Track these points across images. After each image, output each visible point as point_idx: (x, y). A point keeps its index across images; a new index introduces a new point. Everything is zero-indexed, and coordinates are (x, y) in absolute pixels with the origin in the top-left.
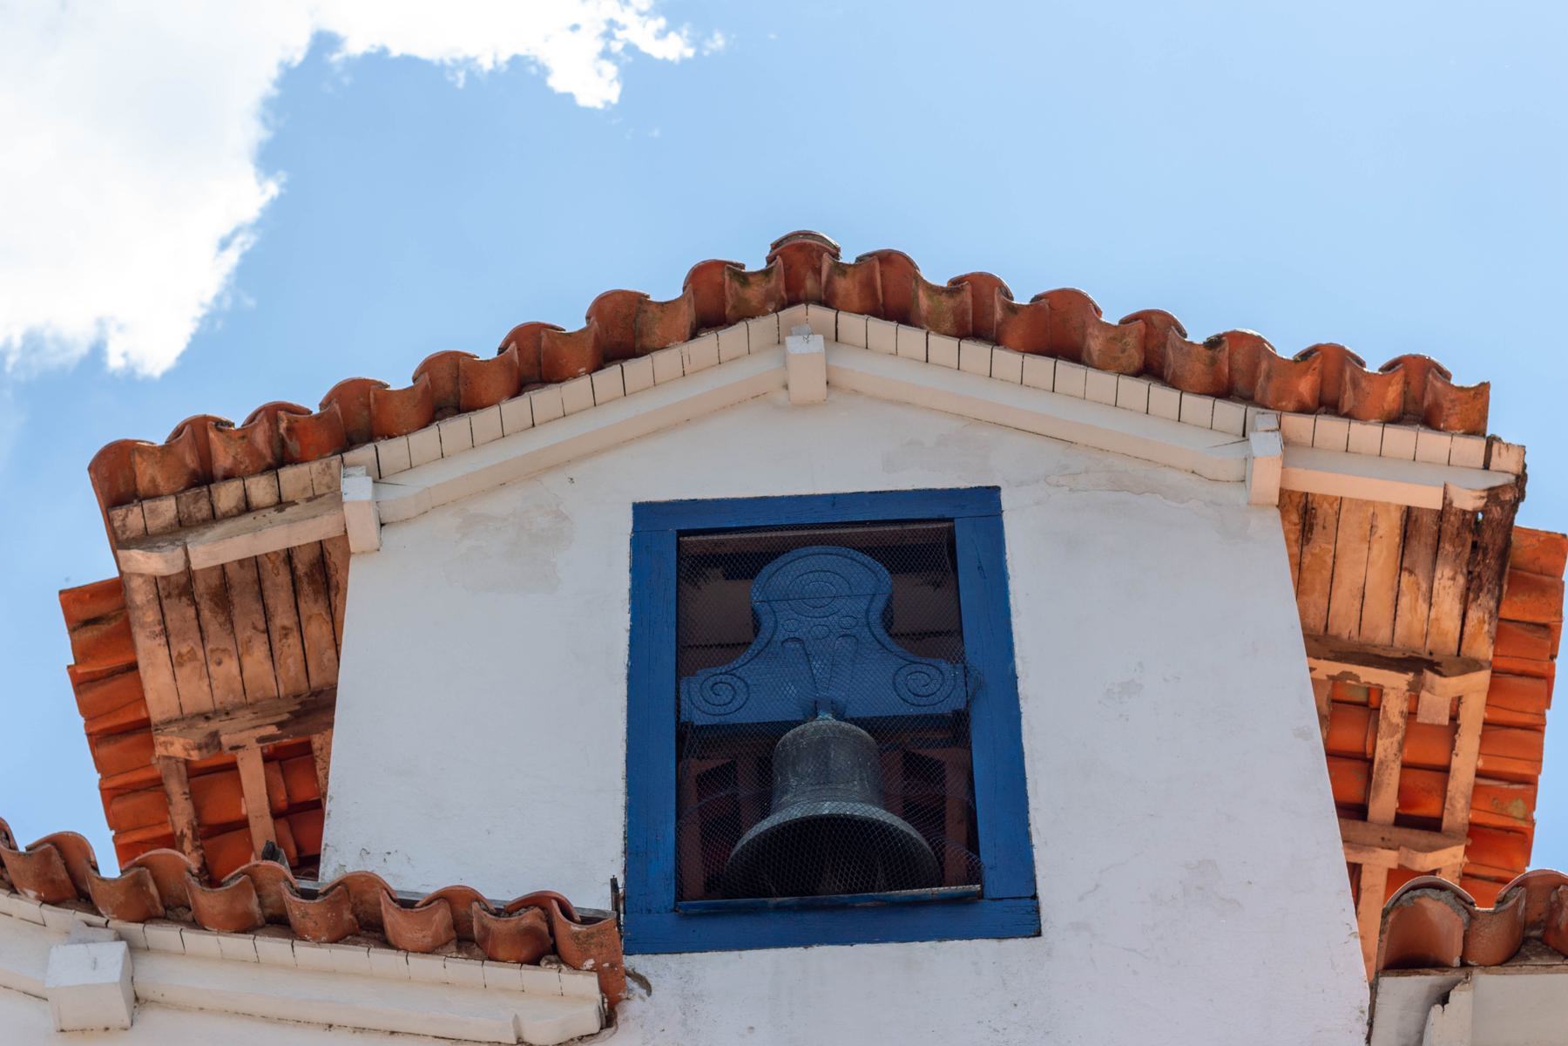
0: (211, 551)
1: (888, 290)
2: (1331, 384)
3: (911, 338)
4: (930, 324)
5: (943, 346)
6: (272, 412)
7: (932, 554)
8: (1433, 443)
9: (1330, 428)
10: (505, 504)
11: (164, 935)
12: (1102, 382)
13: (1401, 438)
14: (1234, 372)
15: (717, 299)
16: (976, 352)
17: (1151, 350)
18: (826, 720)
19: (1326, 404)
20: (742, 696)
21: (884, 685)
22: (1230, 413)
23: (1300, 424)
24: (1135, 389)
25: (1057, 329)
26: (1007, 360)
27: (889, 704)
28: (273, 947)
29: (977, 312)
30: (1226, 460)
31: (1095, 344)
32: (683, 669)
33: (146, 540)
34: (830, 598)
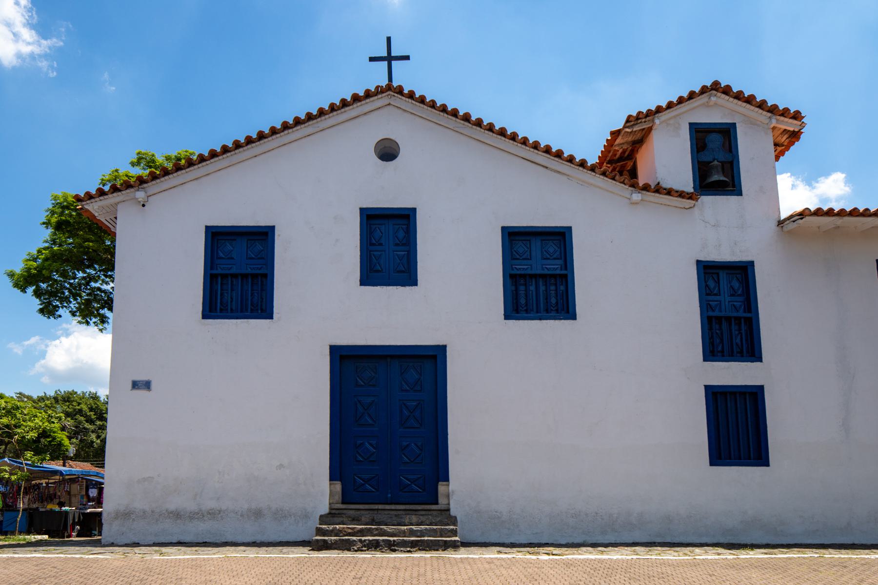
0: (636, 128)
1: (727, 91)
2: (785, 113)
3: (727, 97)
4: (731, 96)
5: (731, 99)
6: (649, 110)
7: (727, 132)
8: (795, 122)
9: (782, 118)
10: (672, 122)
11: (644, 192)
12: (752, 108)
13: (791, 121)
14: (773, 110)
15: (704, 90)
16: (736, 101)
17: (762, 105)
18: (716, 163)
19: (782, 115)
20: (706, 157)
21: (722, 156)
22: (769, 114)
23: (778, 117)
24: (757, 109)
25: (750, 100)
26: (740, 103)
27: (723, 160)
28: (657, 195)
29: (739, 96)
30: (767, 121)
31: (754, 103)
32: (698, 152)
33: (628, 127)
34: (715, 140)
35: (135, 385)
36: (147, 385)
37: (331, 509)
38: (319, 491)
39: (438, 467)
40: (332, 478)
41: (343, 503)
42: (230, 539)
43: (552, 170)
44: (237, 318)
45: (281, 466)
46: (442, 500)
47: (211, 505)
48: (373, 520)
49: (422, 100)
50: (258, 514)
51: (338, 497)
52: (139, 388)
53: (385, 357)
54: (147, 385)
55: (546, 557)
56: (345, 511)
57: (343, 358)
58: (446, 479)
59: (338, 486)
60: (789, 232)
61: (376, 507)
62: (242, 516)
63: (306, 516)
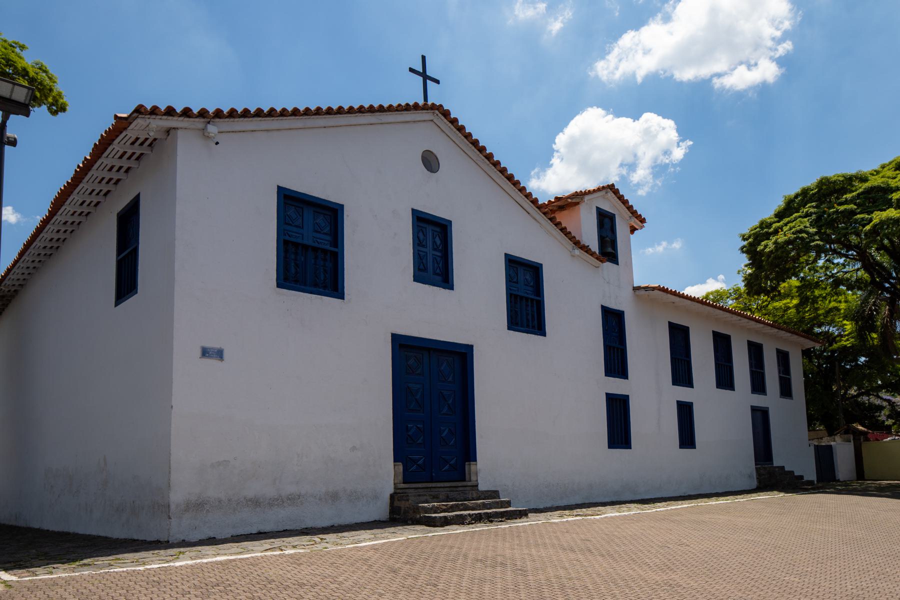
35: (205, 353)
36: (219, 354)
37: (395, 488)
38: (384, 474)
39: (468, 452)
40: (396, 459)
41: (404, 483)
42: (309, 524)
43: (532, 216)
44: (311, 293)
45: (354, 448)
46: (473, 478)
47: (289, 489)
48: (448, 497)
49: (461, 129)
50: (334, 497)
51: (401, 478)
52: (210, 357)
53: (429, 350)
54: (219, 354)
55: (570, 519)
56: (407, 491)
57: (401, 346)
58: (476, 461)
59: (400, 467)
60: (637, 296)
61: (434, 485)
62: (320, 499)
63: (376, 497)
